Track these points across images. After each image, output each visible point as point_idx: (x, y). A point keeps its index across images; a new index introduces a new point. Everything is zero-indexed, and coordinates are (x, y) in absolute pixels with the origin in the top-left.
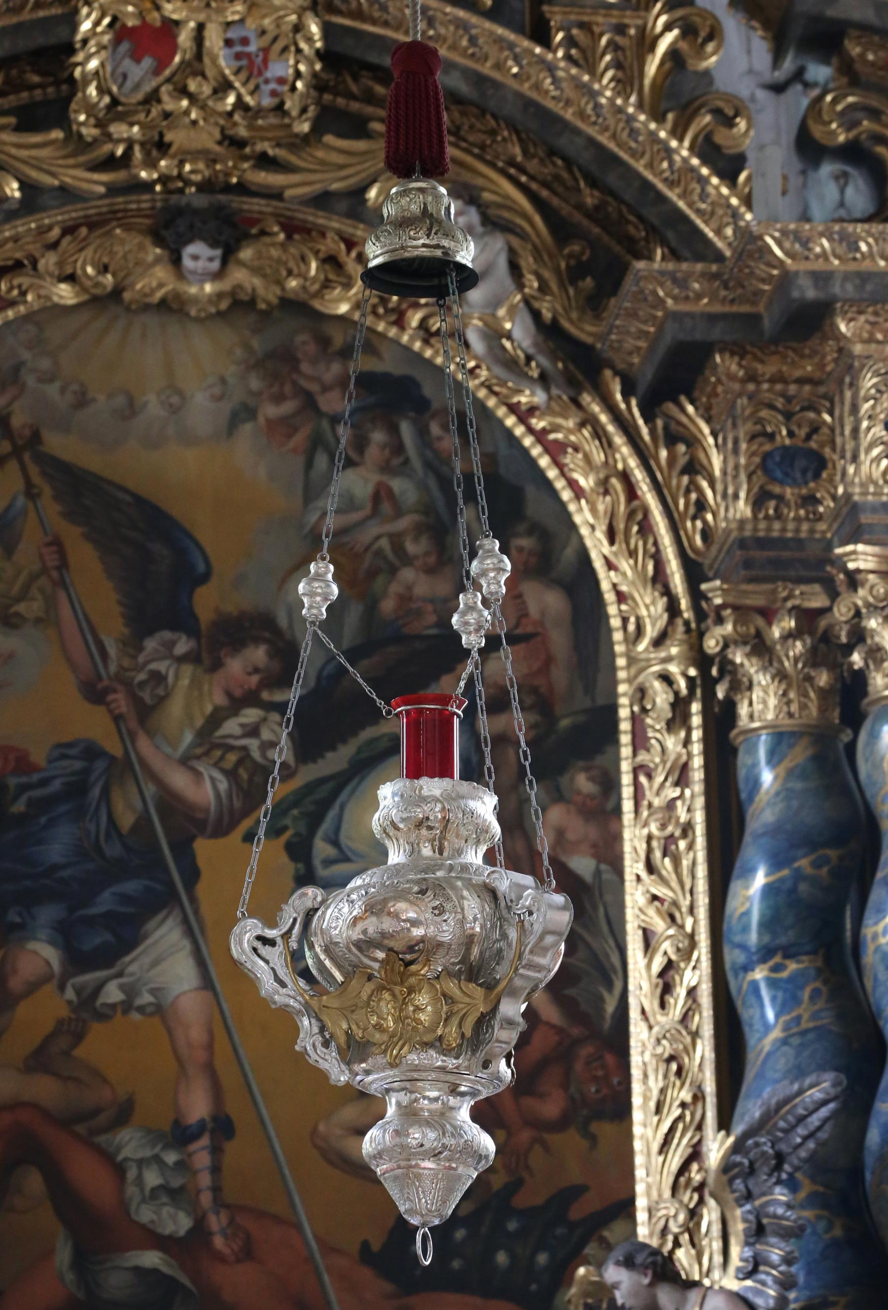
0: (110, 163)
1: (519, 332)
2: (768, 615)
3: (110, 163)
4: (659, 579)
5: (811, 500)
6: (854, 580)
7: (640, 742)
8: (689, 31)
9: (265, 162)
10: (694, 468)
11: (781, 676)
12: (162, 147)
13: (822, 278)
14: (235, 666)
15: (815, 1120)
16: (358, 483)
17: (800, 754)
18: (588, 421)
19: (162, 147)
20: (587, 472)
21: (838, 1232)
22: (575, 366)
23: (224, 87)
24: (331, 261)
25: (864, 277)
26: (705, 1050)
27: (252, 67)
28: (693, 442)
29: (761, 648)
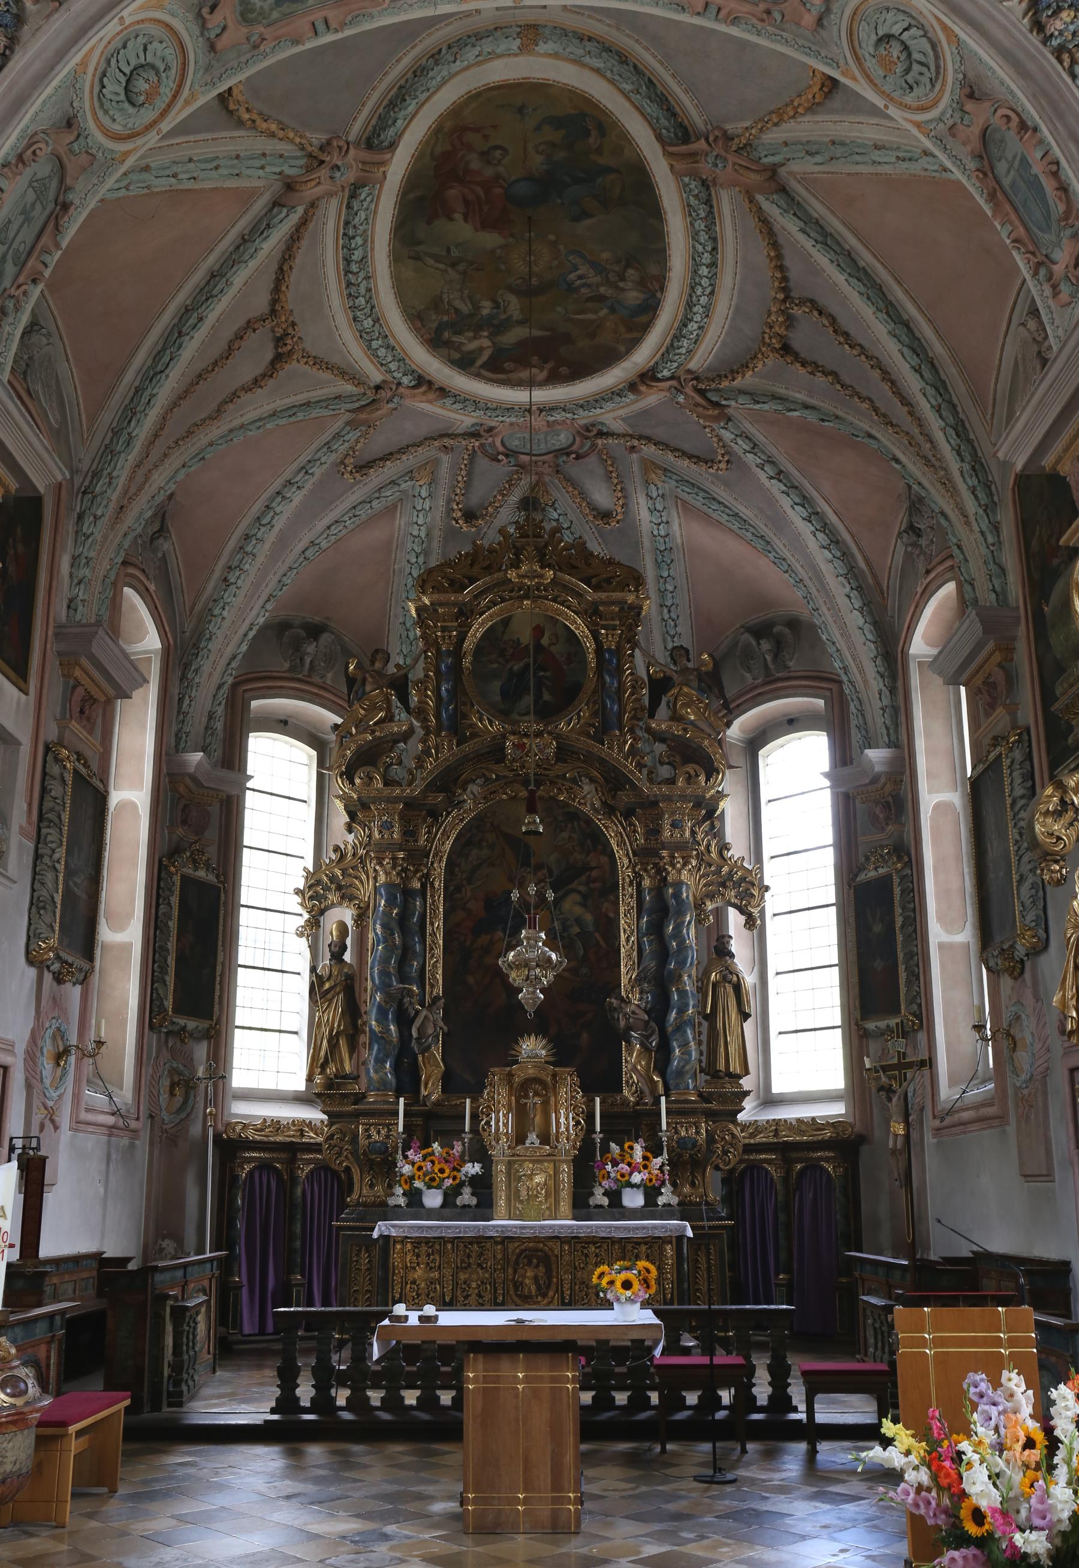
0: (513, 770)
1: (597, 804)
2: (648, 864)
3: (513, 770)
4: (628, 855)
5: (657, 840)
6: (664, 857)
7: (623, 889)
8: (634, 739)
9: (545, 769)
10: (635, 831)
11: (650, 877)
12: (524, 767)
13: (656, 796)
14: (539, 874)
16: (565, 835)
17: (653, 893)
18: (613, 821)
19: (524, 767)
20: (612, 833)
22: (609, 810)
23: (536, 755)
24: (559, 789)
25: (664, 795)
26: (635, 953)
27: (541, 751)
28: (635, 826)
29: (646, 870)
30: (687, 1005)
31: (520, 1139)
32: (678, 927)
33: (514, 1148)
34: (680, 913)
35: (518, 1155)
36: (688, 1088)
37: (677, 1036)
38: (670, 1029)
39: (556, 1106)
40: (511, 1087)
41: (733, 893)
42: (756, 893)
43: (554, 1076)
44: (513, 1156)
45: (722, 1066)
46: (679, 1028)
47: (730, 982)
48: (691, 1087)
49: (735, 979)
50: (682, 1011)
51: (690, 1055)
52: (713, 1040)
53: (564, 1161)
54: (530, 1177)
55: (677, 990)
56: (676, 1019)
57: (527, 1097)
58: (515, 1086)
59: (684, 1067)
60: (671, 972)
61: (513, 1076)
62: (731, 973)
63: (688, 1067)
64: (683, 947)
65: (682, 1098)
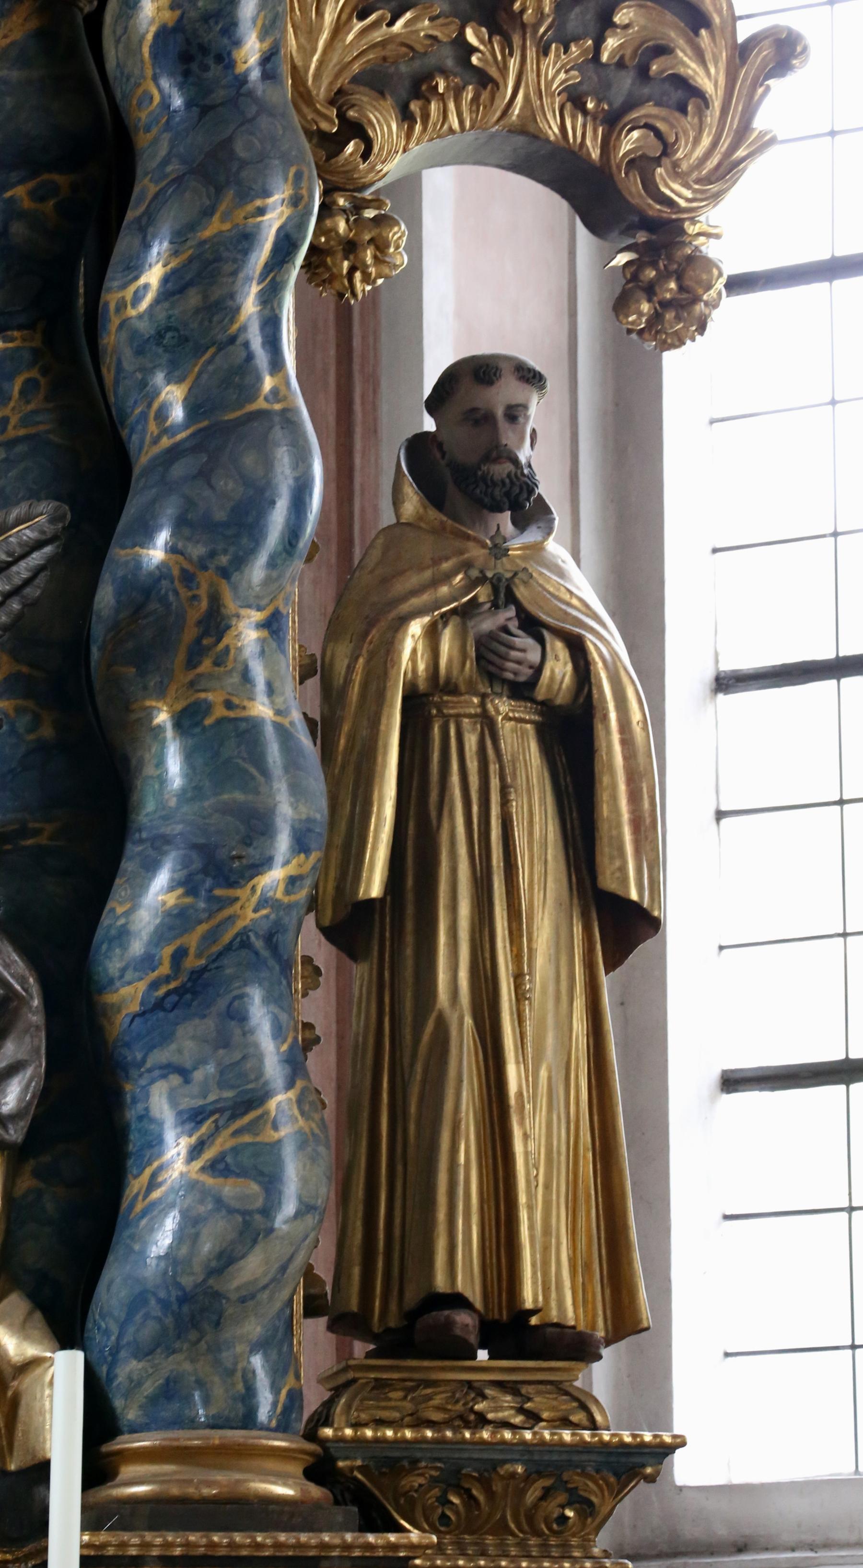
15: (22, 570)
21: (47, 732)
30: (257, 825)
32: (205, 275)
34: (221, 172)
36: (248, 1420)
37: (187, 1041)
38: (128, 995)
41: (556, 71)
42: (709, 80)
45: (457, 1264)
46: (196, 987)
47: (522, 690)
48: (265, 1405)
49: (559, 669)
50: (219, 868)
51: (271, 1181)
52: (395, 1099)
55: (188, 720)
56: (177, 921)
59: (226, 1259)
60: (144, 591)
62: (532, 625)
63: (253, 1266)
64: (229, 421)
65: (212, 1483)
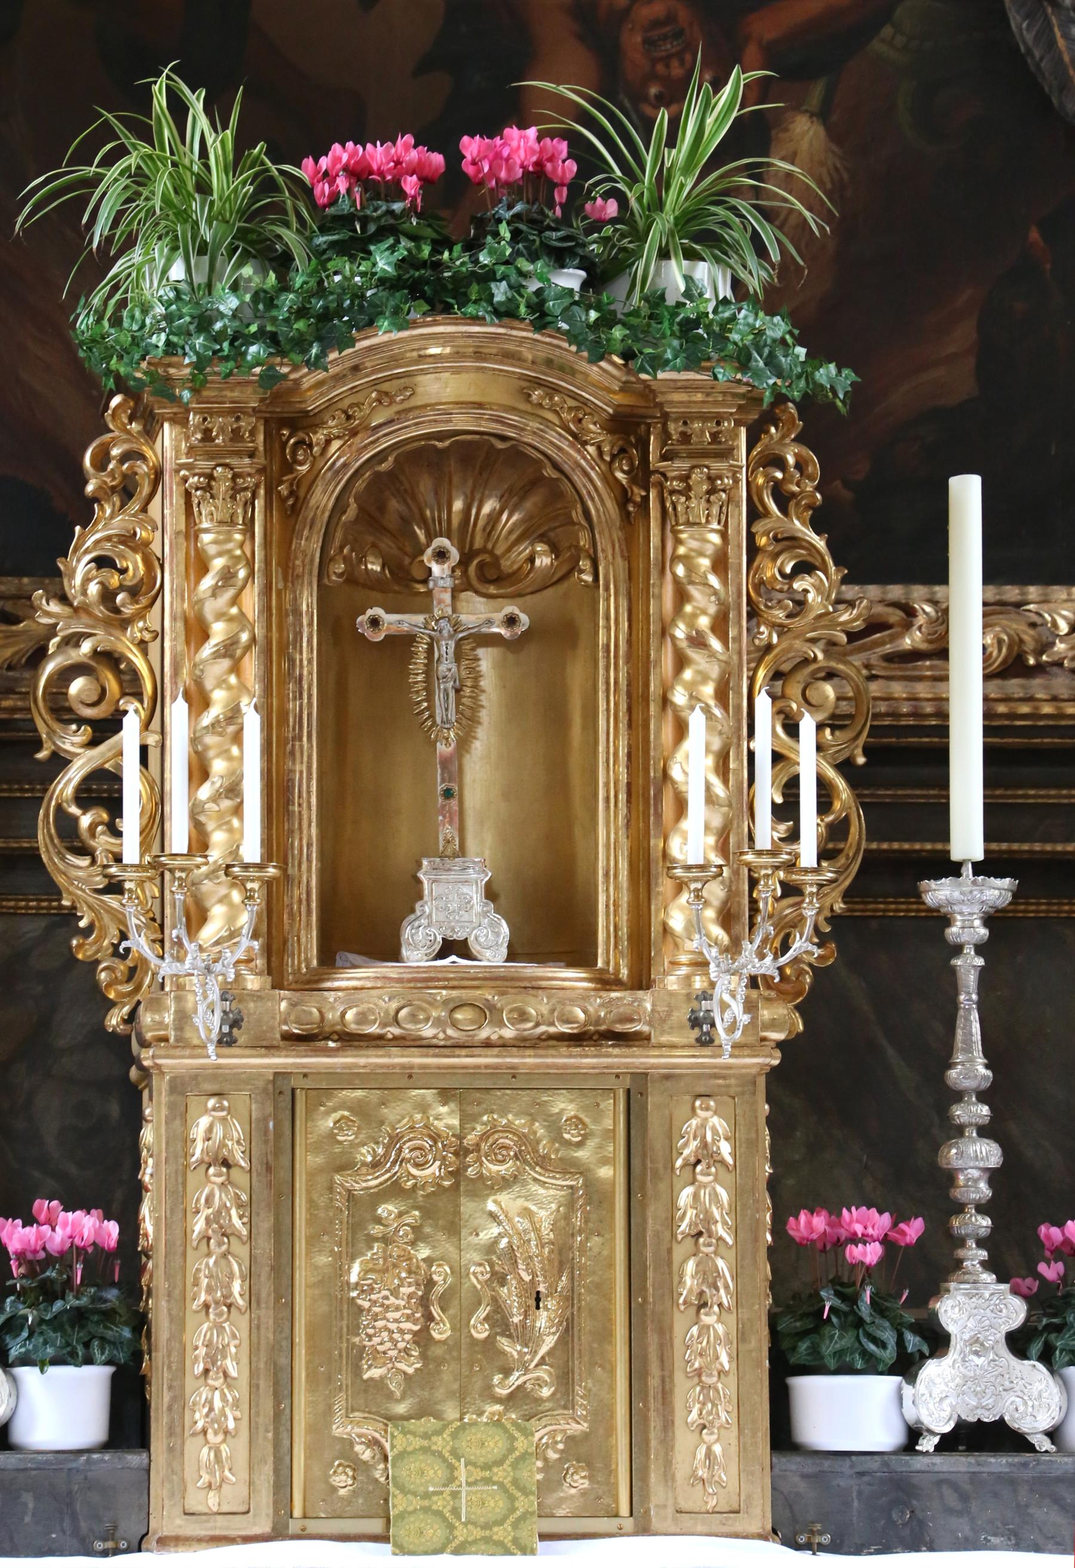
31: (360, 919)
33: (311, 983)
35: (349, 1040)
39: (640, 663)
40: (290, 510)
43: (629, 428)
44: (305, 1040)
53: (704, 1089)
54: (443, 1209)
57: (405, 585)
58: (322, 498)
61: (303, 422)
